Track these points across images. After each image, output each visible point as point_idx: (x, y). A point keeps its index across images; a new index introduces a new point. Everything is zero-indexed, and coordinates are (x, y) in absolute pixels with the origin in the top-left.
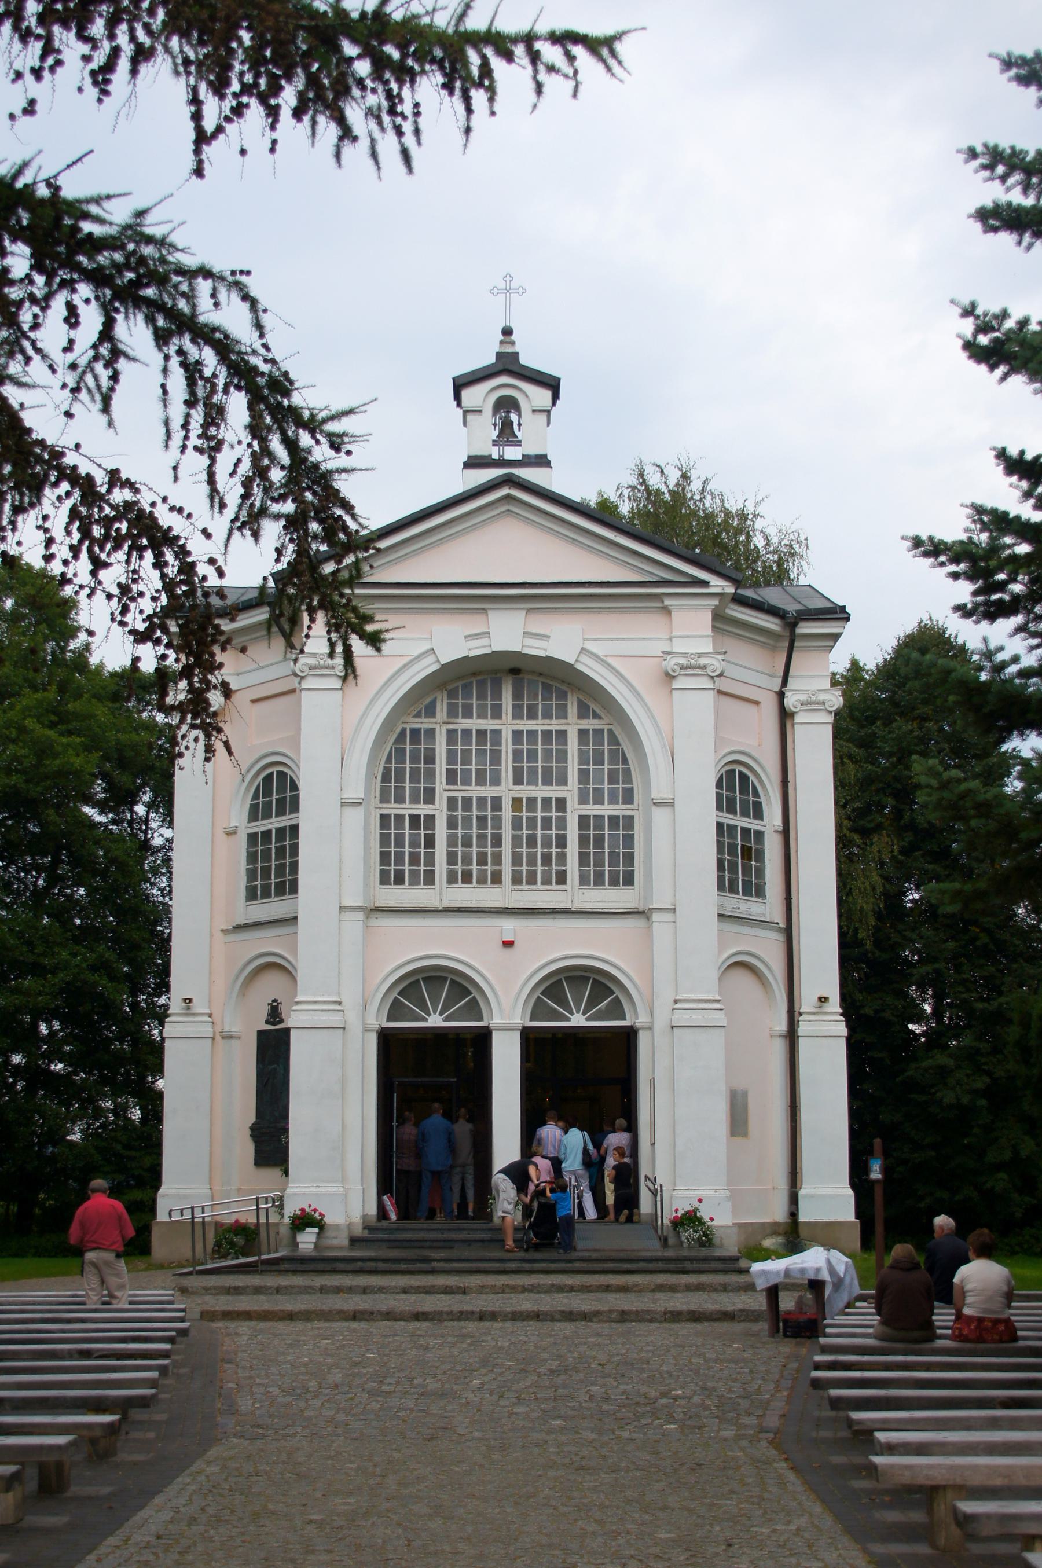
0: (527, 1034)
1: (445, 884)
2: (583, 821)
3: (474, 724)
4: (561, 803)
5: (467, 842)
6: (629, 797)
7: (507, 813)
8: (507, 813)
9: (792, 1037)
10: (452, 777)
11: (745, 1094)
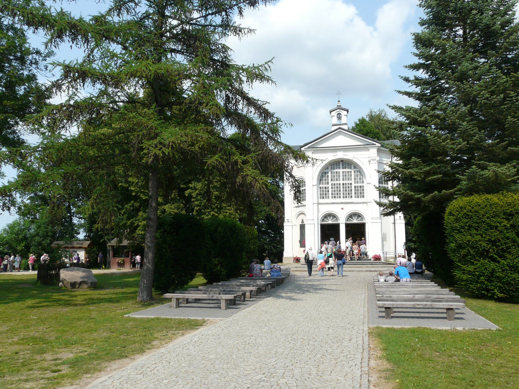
2: (355, 187)
4: (351, 184)
5: (335, 191)
6: (363, 182)
7: (341, 186)
8: (341, 186)
10: (332, 180)
11: (386, 234)
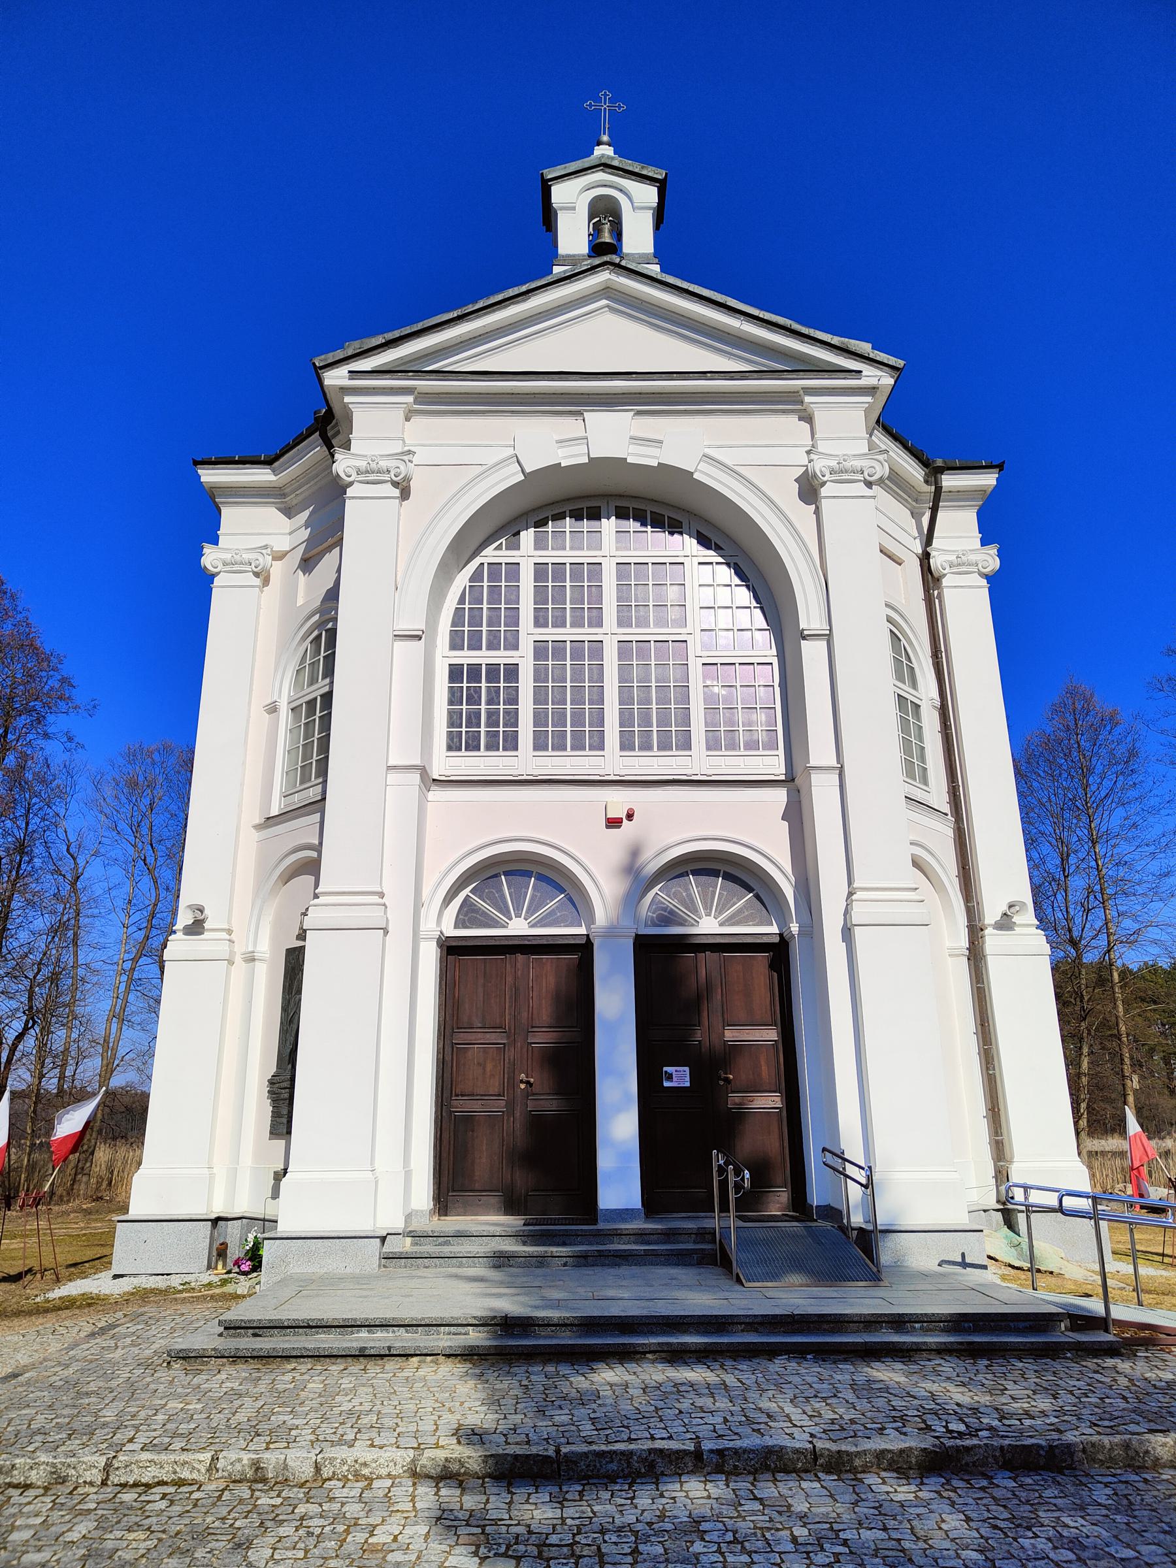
9: (976, 956)
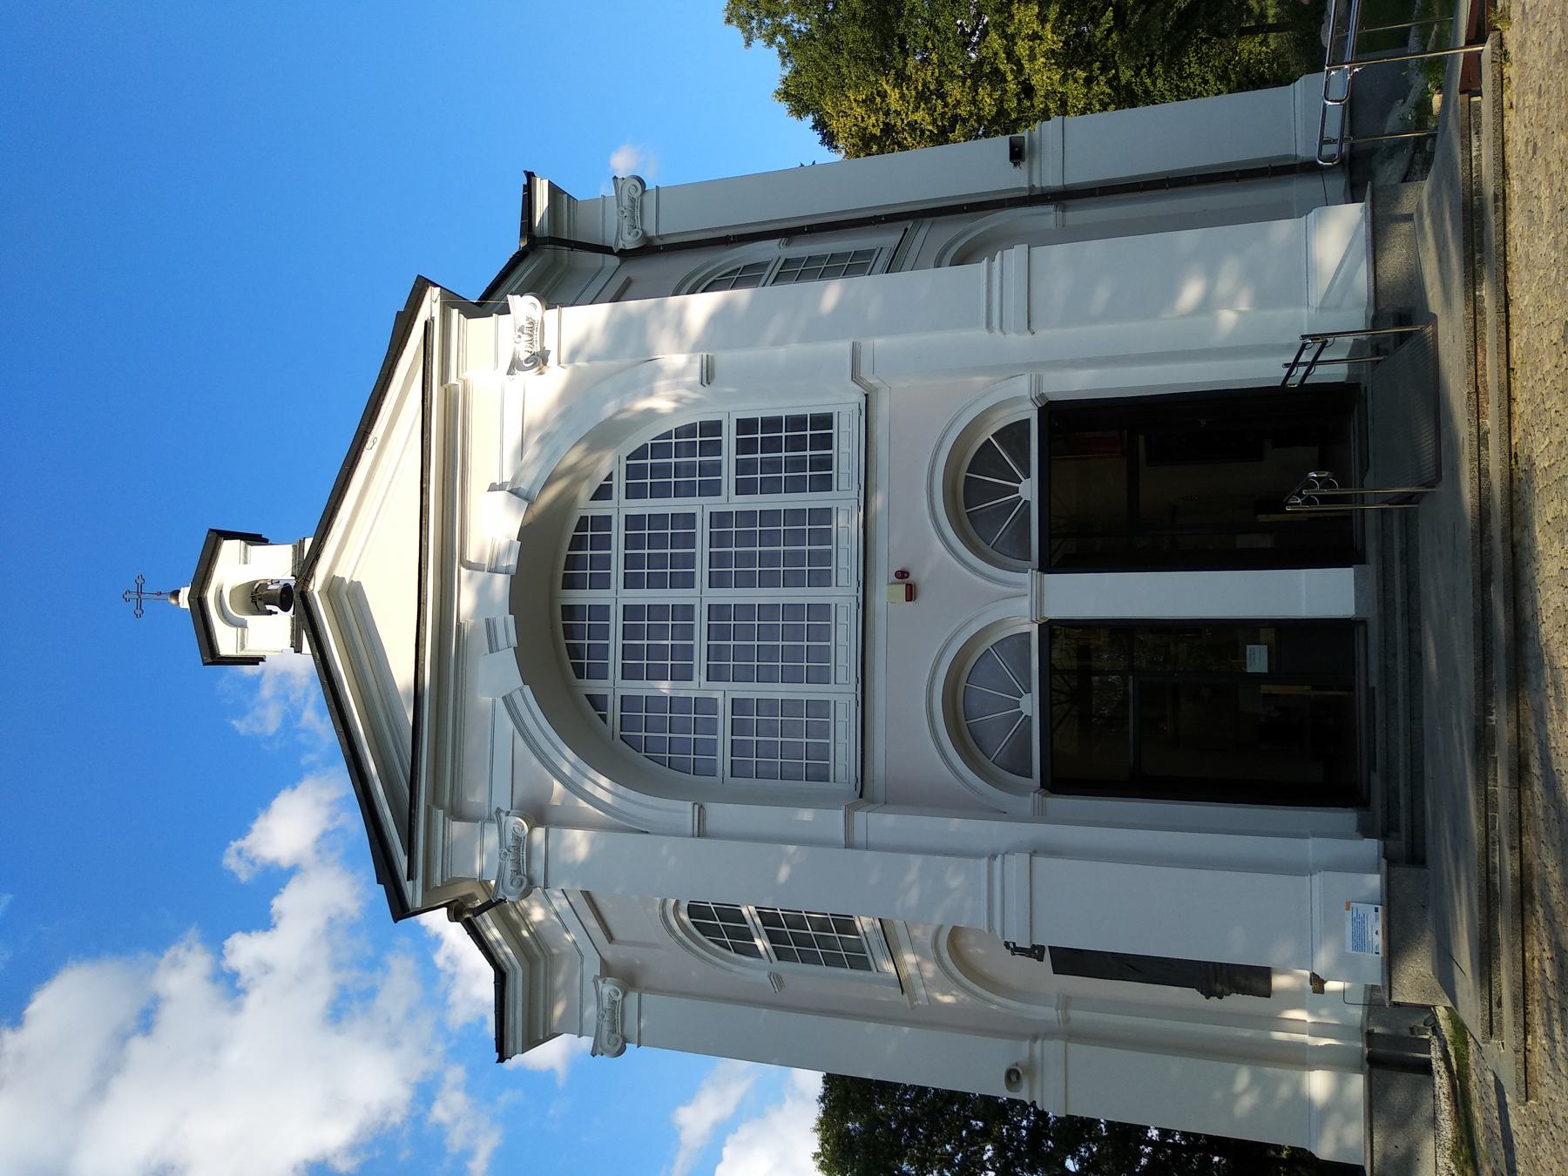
0: (1050, 564)
1: (830, 687)
3: (615, 642)
4: (719, 519)
